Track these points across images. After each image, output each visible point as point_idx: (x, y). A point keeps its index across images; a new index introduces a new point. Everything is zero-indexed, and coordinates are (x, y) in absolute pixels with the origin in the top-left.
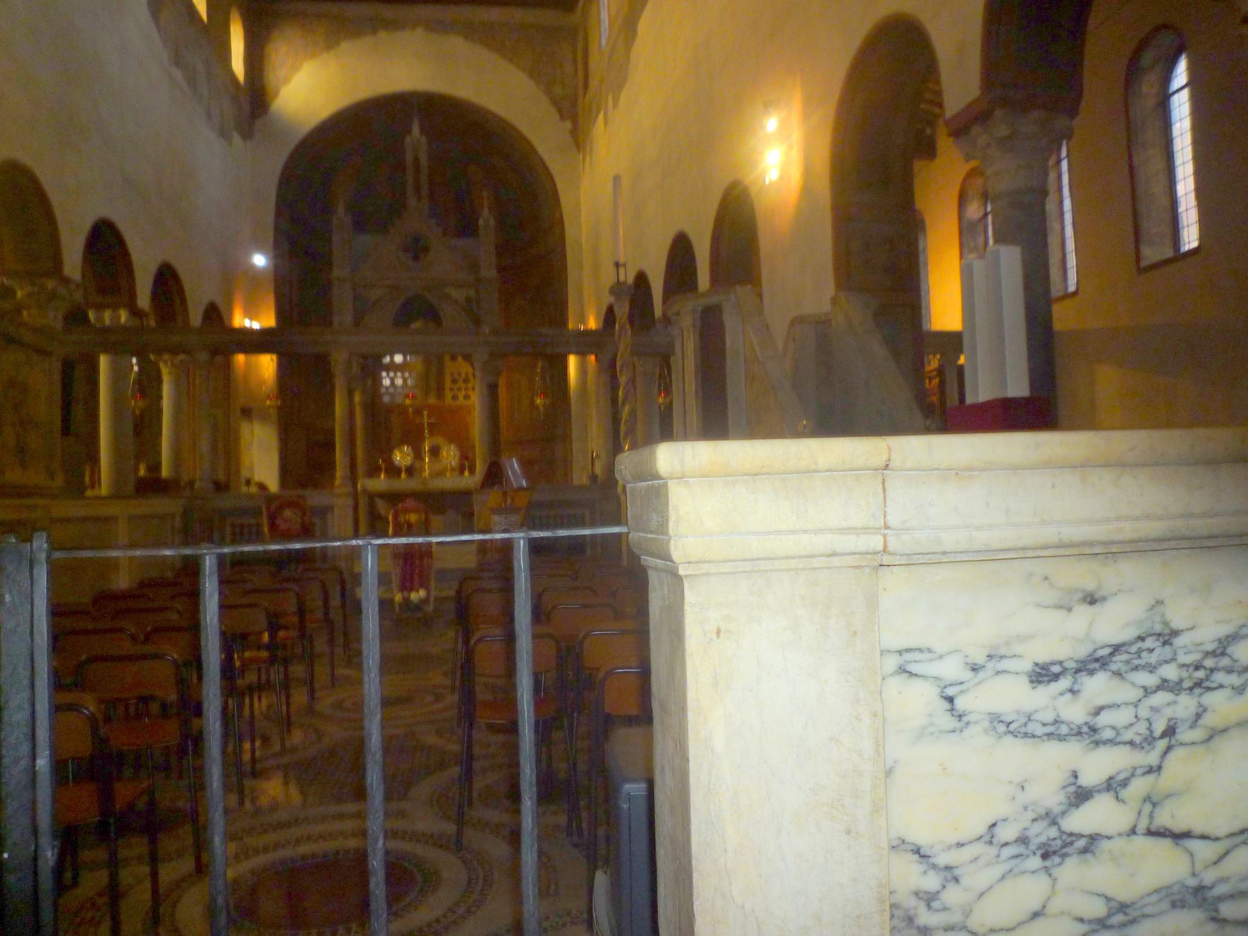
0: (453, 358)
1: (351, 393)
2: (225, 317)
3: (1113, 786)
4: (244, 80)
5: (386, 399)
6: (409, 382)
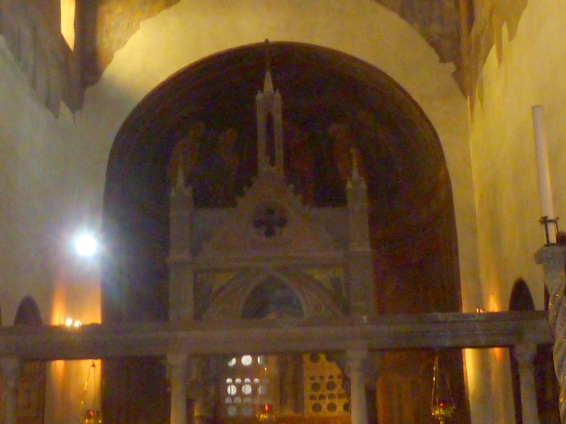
0: (314, 358)
1: (189, 404)
2: (43, 316)
4: (76, 46)
5: (232, 412)
6: (260, 390)
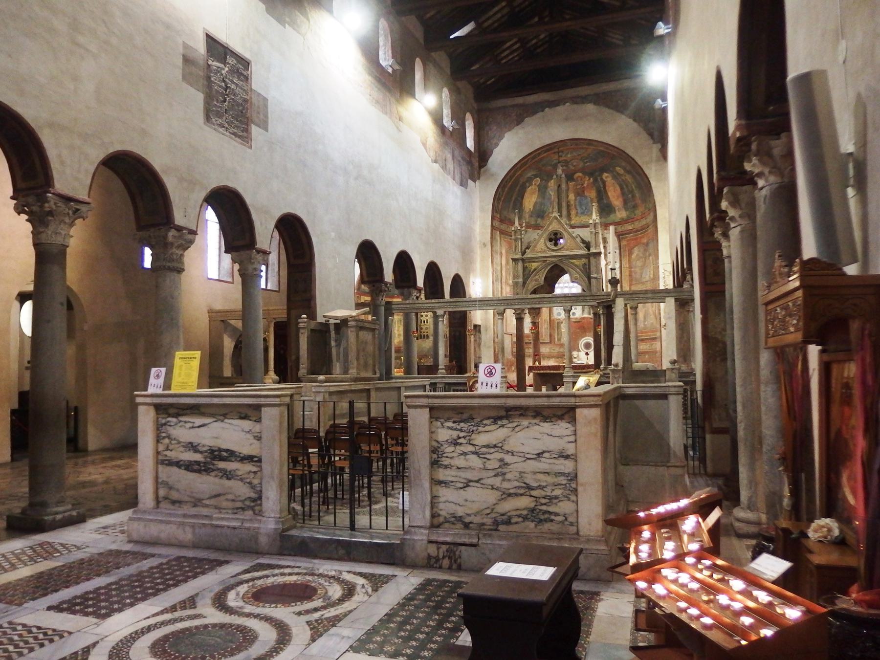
3: (464, 437)
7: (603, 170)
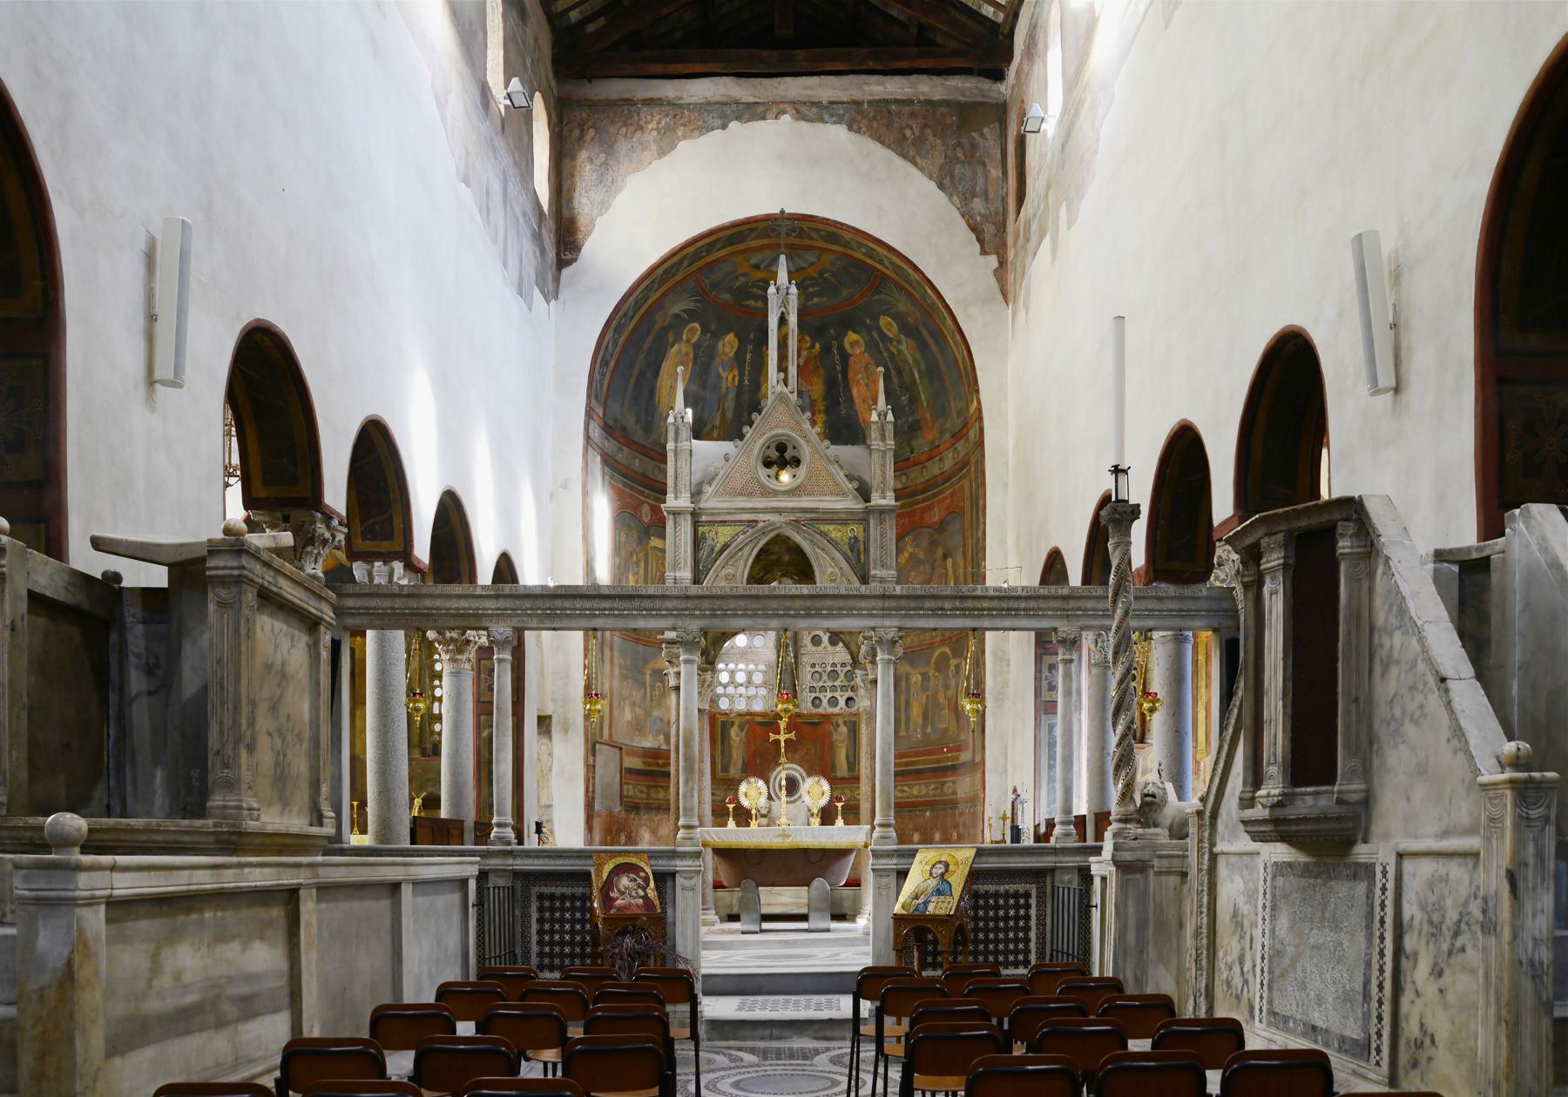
7: (848, 323)
